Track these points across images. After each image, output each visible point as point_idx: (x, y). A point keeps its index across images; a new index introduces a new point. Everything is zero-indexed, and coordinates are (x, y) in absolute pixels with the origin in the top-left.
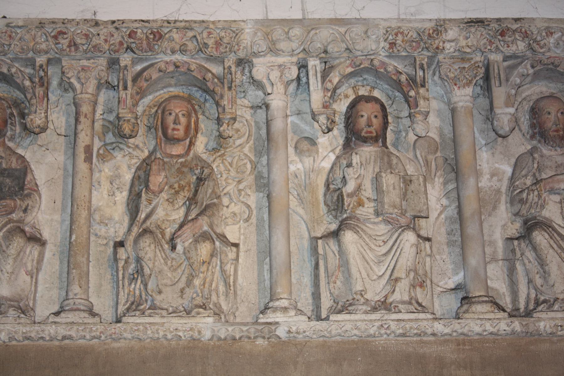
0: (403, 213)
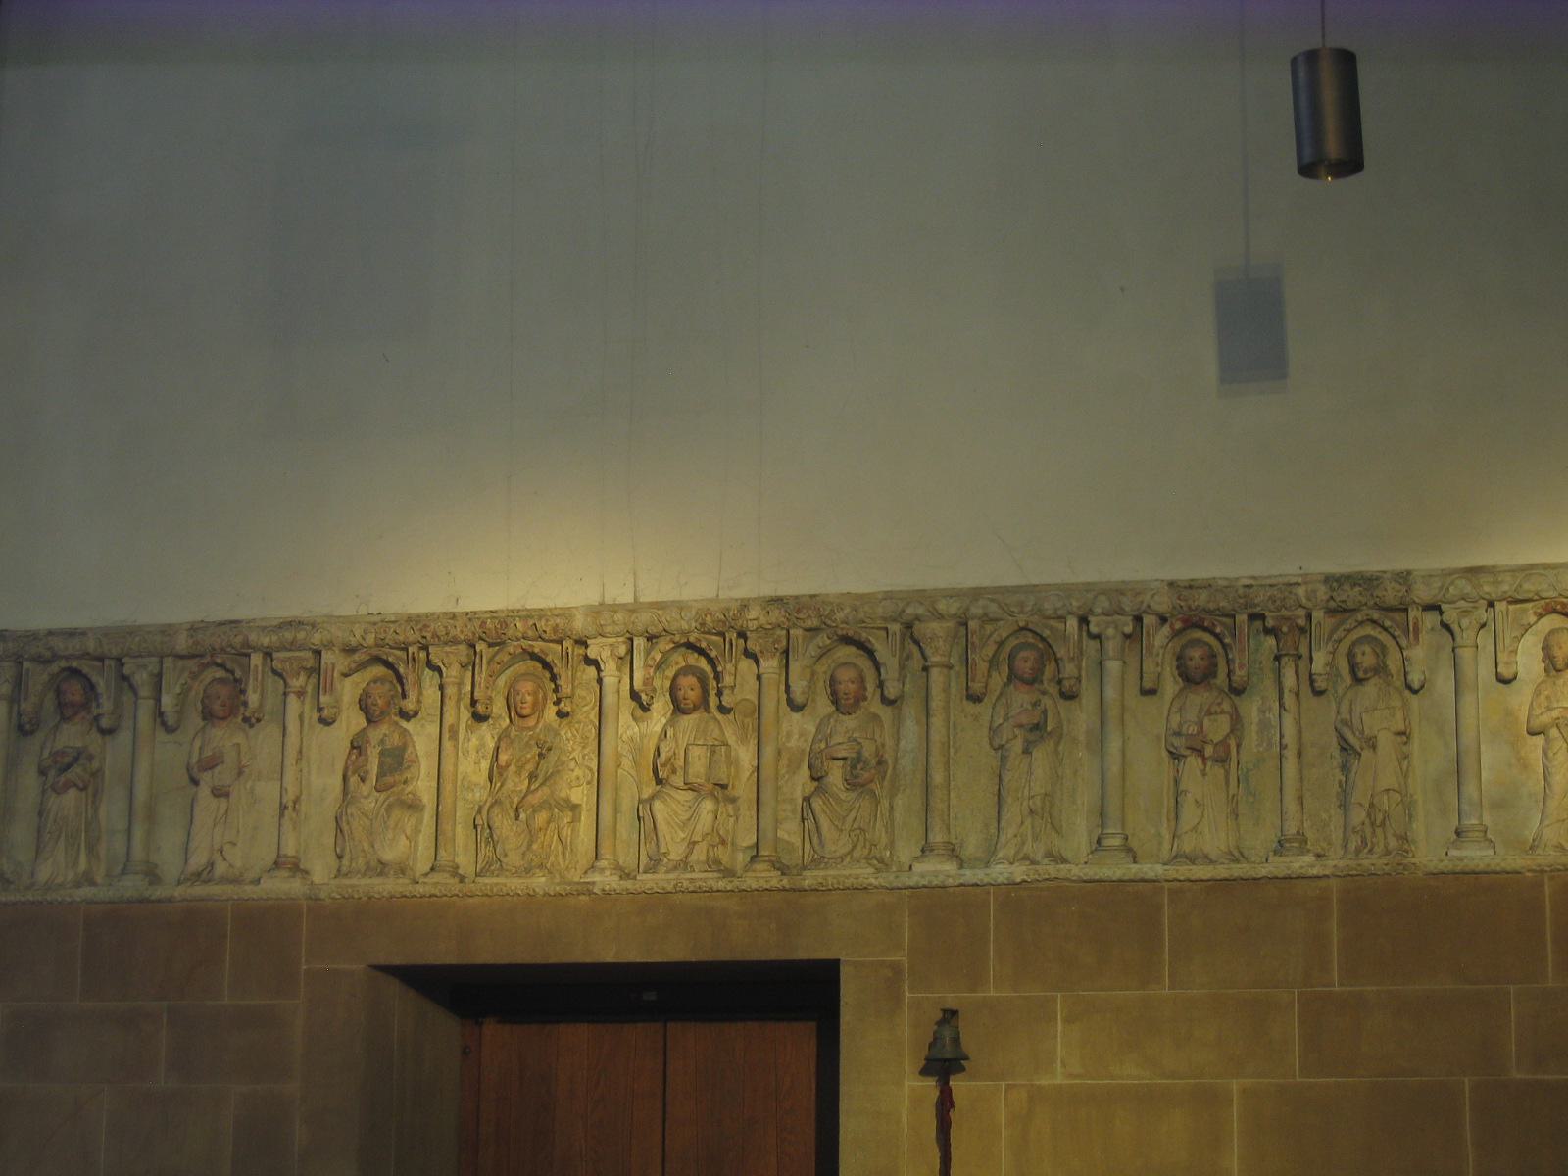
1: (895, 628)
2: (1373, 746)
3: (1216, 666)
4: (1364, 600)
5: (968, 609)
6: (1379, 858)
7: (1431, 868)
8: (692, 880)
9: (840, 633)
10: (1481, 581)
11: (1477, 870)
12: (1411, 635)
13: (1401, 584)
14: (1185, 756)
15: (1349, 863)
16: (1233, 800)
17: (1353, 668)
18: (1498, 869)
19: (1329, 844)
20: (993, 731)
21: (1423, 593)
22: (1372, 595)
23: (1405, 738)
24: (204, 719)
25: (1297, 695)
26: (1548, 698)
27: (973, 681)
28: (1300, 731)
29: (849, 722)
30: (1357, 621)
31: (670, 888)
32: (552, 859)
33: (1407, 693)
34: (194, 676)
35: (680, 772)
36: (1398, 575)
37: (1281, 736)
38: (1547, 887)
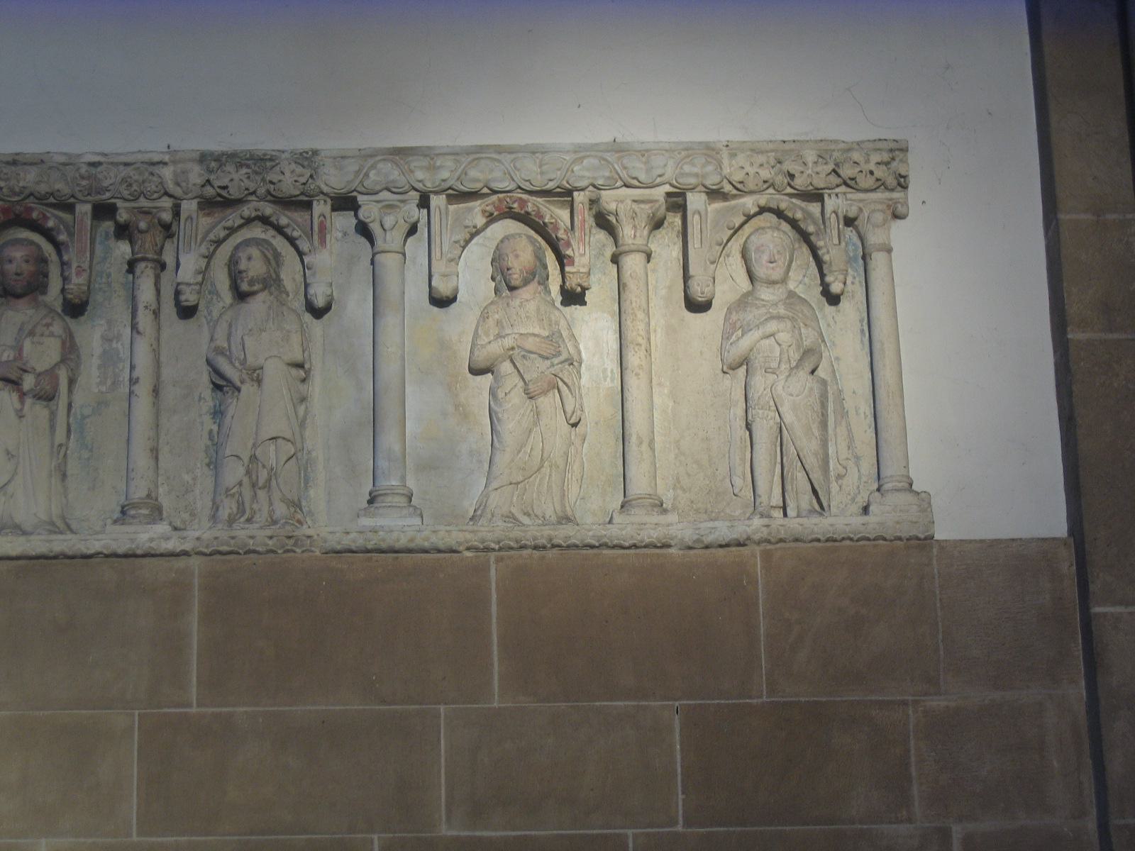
3: (46, 275)
4: (252, 186)
6: (261, 528)
7: (334, 542)
10: (412, 165)
11: (398, 546)
12: (316, 237)
13: (303, 167)
15: (218, 534)
16: (60, 452)
17: (235, 276)
18: (426, 544)
19: (193, 515)
21: (334, 180)
22: (263, 180)
23: (302, 373)
25: (156, 313)
26: (499, 323)
28: (158, 364)
30: (242, 218)
33: (308, 317)
36: (301, 154)
37: (132, 368)
38: (493, 572)
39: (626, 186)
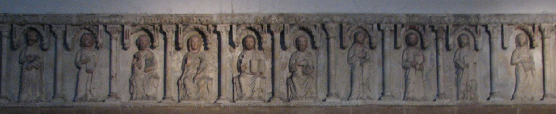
0: (258, 71)
1: (319, 25)
2: (467, 66)
5: (343, 19)
8: (254, 103)
9: (301, 26)
14: (410, 68)
20: (349, 59)
21: (483, 21)
24: (81, 46)
25: (443, 51)
27: (345, 42)
29: (302, 55)
31: (247, 105)
32: (205, 95)
34: (78, 32)
35: (248, 69)
37: (438, 63)
39: (547, 23)
